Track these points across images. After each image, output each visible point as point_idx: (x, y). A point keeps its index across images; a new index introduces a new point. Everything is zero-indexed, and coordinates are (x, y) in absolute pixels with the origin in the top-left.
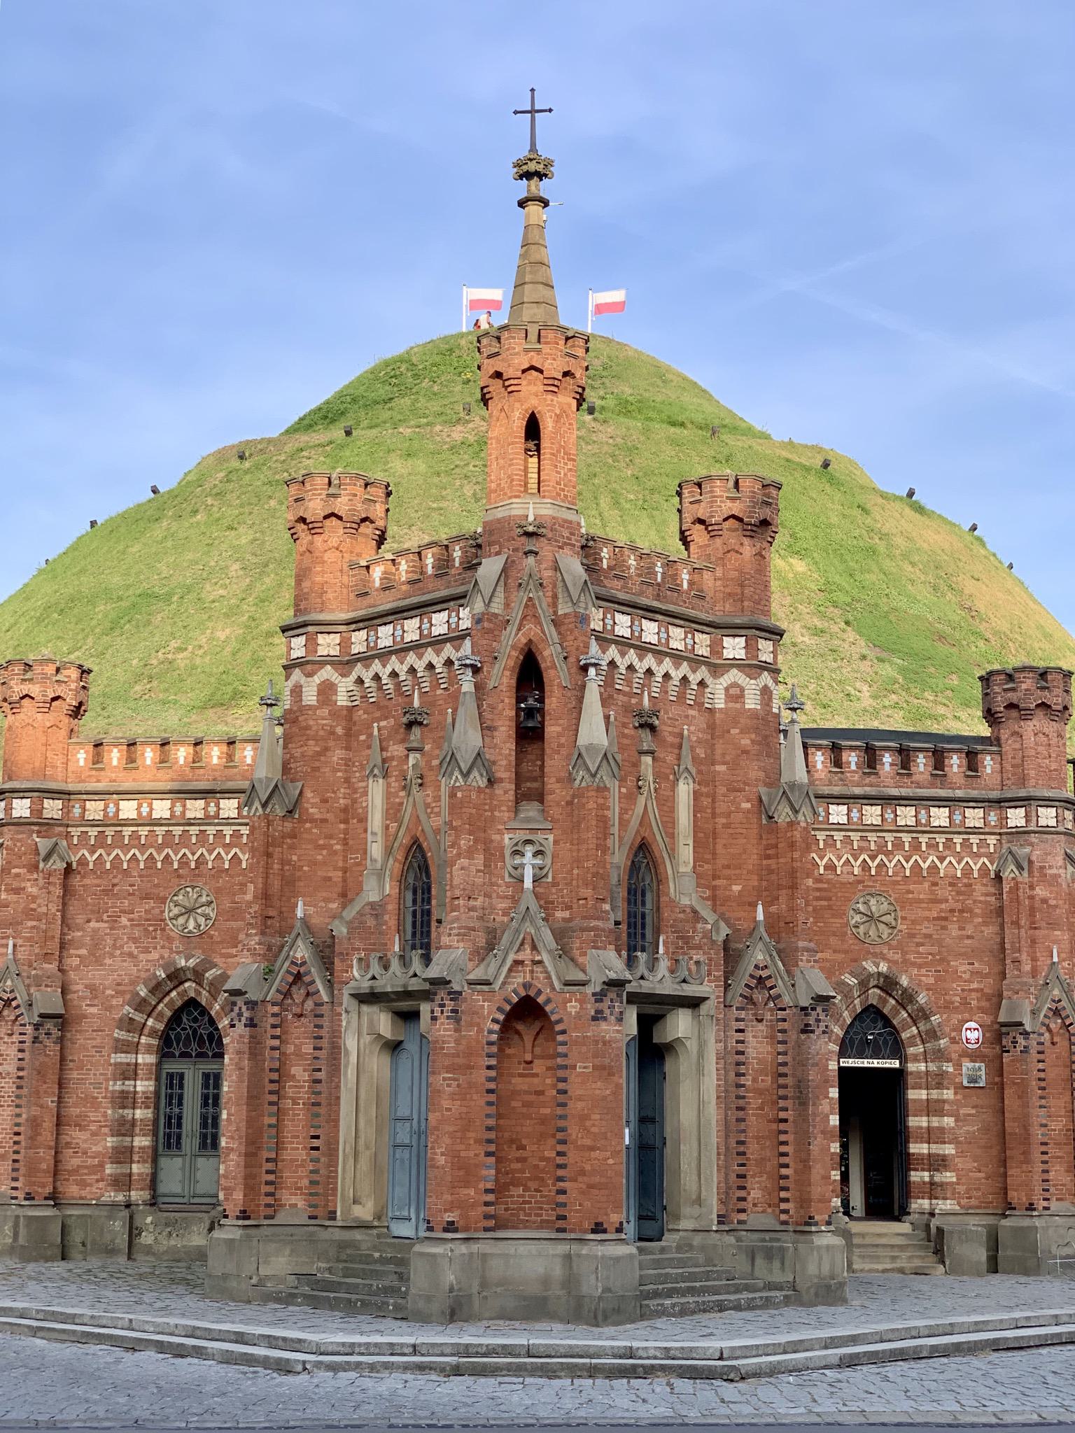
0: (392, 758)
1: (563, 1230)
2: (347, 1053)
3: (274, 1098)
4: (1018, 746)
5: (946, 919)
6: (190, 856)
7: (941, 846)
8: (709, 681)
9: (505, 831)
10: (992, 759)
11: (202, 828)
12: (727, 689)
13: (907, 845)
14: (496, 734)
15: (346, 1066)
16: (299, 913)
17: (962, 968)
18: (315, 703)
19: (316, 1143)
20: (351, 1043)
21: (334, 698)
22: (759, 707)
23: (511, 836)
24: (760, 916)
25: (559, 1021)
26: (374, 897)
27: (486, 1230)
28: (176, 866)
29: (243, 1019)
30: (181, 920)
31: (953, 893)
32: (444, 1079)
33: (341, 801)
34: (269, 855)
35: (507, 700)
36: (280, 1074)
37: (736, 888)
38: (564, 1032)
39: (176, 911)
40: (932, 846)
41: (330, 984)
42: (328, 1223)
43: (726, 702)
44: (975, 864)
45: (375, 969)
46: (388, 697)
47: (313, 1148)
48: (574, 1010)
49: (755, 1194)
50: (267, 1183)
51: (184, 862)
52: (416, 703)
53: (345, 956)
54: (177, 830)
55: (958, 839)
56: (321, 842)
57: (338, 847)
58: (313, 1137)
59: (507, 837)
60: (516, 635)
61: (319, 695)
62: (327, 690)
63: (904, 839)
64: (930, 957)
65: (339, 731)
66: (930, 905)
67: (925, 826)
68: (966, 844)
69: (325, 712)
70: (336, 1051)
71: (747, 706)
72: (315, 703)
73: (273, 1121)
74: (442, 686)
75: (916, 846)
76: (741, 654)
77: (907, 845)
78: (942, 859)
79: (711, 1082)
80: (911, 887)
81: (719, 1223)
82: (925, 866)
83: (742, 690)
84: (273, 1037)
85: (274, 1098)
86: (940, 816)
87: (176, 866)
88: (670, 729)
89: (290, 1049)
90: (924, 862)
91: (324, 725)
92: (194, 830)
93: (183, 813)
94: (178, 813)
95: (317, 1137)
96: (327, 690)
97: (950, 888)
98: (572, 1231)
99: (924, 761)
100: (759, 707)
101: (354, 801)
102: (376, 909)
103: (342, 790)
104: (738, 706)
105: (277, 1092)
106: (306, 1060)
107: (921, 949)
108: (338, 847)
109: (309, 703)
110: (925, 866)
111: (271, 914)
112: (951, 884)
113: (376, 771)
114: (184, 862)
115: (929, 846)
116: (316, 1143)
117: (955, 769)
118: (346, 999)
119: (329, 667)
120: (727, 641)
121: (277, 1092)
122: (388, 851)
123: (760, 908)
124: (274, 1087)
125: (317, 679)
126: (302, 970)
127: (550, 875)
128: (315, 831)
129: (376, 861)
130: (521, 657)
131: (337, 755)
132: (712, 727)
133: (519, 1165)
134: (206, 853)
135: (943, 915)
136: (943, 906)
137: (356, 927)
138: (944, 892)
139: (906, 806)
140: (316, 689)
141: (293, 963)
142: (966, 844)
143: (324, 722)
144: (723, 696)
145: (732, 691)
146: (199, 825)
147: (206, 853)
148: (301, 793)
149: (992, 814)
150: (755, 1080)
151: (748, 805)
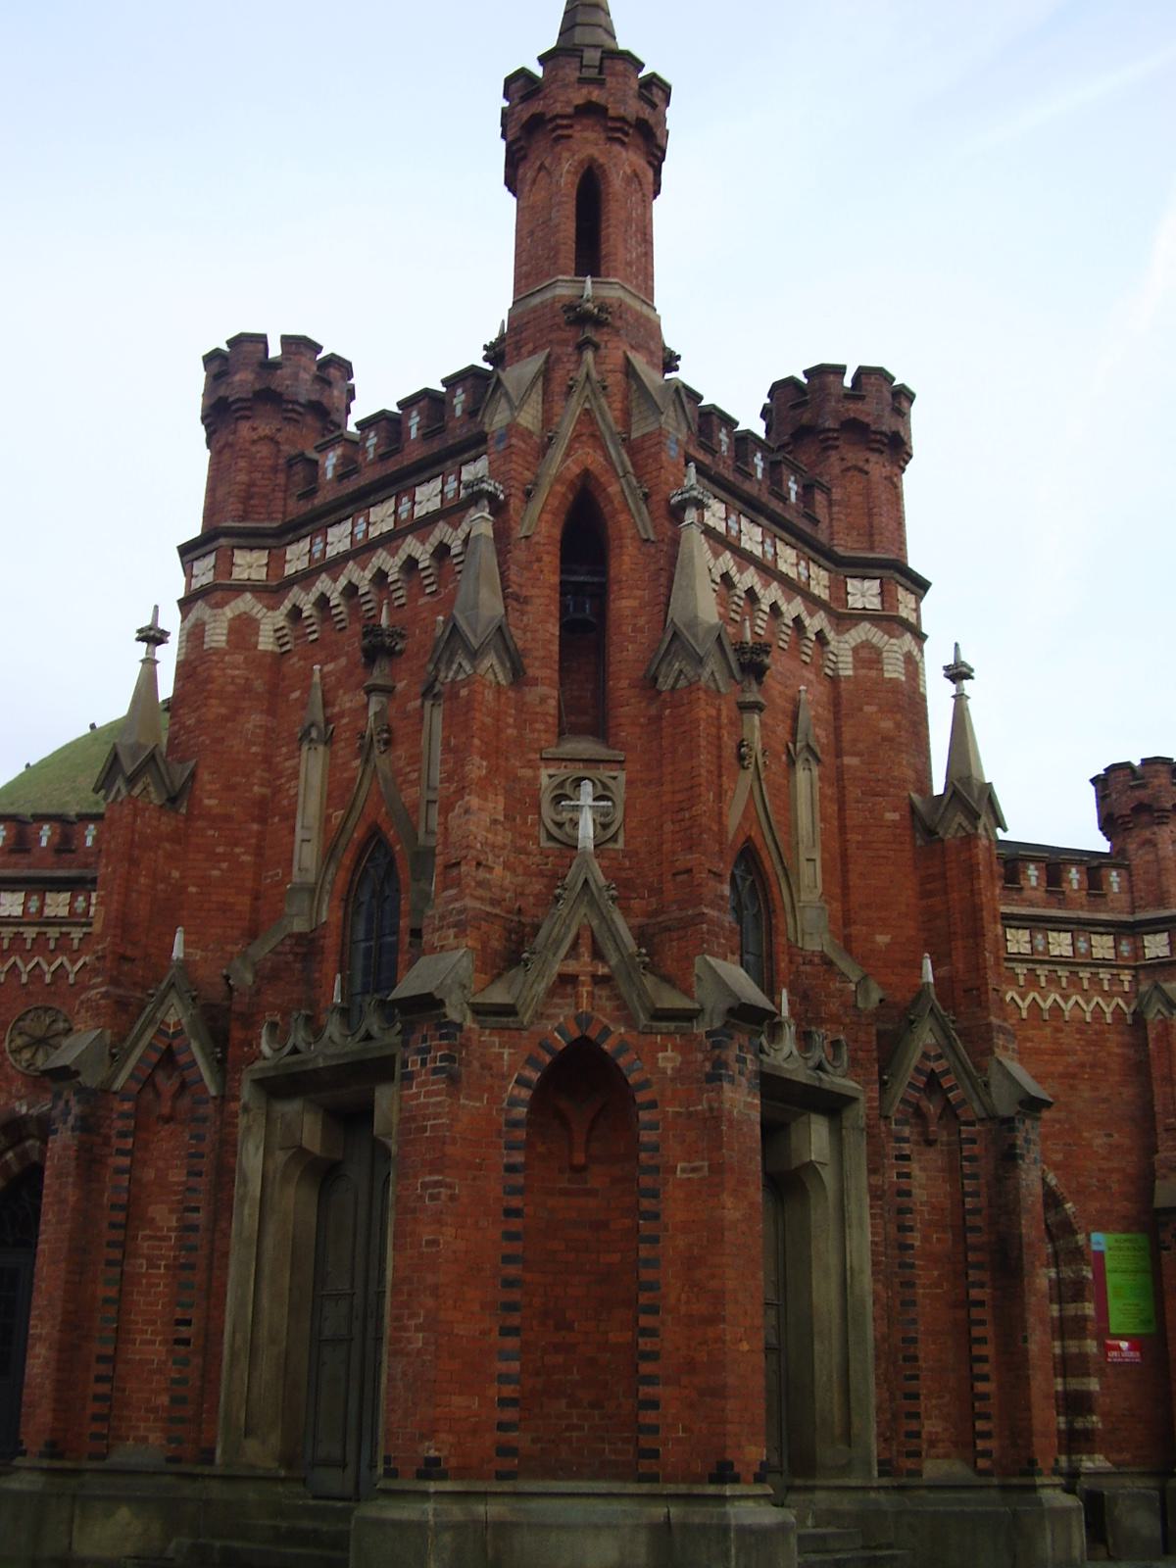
0: (341, 715)
1: (653, 1478)
2: (245, 1182)
3: (117, 1254)
4: (1151, 857)
5: (1074, 1076)
6: (45, 967)
7: (1064, 980)
8: (830, 635)
9: (542, 764)
10: (1118, 876)
11: (64, 929)
12: (855, 650)
13: (1021, 978)
14: (529, 608)
15: (242, 1201)
16: (178, 952)
18: (223, 645)
19: (184, 1331)
20: (252, 1159)
21: (253, 640)
22: (903, 678)
23: (552, 771)
24: (928, 974)
25: (645, 1084)
26: (299, 926)
27: (501, 1476)
28: (24, 979)
29: (71, 1120)
30: (27, 1055)
31: (1082, 1043)
32: (425, 1186)
33: (256, 788)
34: (134, 862)
35: (546, 558)
36: (132, 1213)
37: (882, 939)
38: (652, 1105)
39: (19, 1041)
40: (1054, 980)
41: (223, 1066)
42: (198, 1470)
43: (855, 668)
44: (1108, 1006)
45: (299, 1036)
46: (339, 626)
47: (177, 1342)
48: (670, 1065)
49: (931, 1426)
50: (97, 1398)
51: (36, 974)
52: (384, 621)
53: (249, 1021)
54: (30, 933)
55: (1085, 974)
56: (220, 850)
57: (246, 858)
58: (179, 1322)
59: (544, 773)
60: (563, 461)
61: (229, 634)
62: (243, 629)
63: (1018, 971)
64: (1058, 1126)
65: (259, 685)
66: (1055, 1058)
67: (1043, 954)
68: (1095, 980)
69: (239, 658)
70: (224, 1174)
71: (887, 675)
72: (223, 645)
73: (112, 1293)
74: (428, 591)
76: (874, 603)
78: (1066, 998)
79: (862, 1240)
80: (1031, 1033)
81: (881, 1474)
82: (1046, 1005)
83: (878, 652)
84: (121, 1152)
85: (117, 1254)
86: (1061, 944)
87: (24, 979)
88: (779, 687)
89: (150, 1174)
90: (1045, 1001)
91: (233, 677)
92: (53, 932)
93: (41, 910)
94: (33, 910)
95: (188, 1323)
96: (243, 629)
97: (1078, 1036)
98: (668, 1479)
99: (1036, 873)
100: (903, 678)
101: (277, 791)
102: (307, 946)
103: (258, 773)
104: (873, 673)
105: (122, 1245)
106: (176, 1193)
108: (246, 858)
109: (214, 645)
110: (1046, 1005)
111: (129, 953)
112: (1080, 1031)
113: (314, 734)
114: (36, 974)
115: (1049, 980)
116: (184, 1331)
118: (246, 1092)
119: (248, 596)
120: (853, 585)
121: (122, 1245)
122: (329, 854)
123: (928, 965)
124: (118, 1235)
125: (229, 612)
126: (176, 1043)
127: (621, 839)
128: (210, 832)
129: (307, 870)
130: (571, 497)
131: (254, 721)
132: (836, 702)
133: (560, 1359)
134: (67, 964)
135: (1070, 1069)
136: (1070, 1059)
137: (269, 976)
138: (1068, 1039)
139: (1018, 928)
140: (226, 625)
141: (161, 1032)
142: (1095, 980)
143: (237, 672)
144: (850, 659)
145: (864, 654)
146: (61, 925)
147: (67, 964)
148: (193, 775)
149: (1124, 942)
150: (926, 1239)
151: (895, 816)
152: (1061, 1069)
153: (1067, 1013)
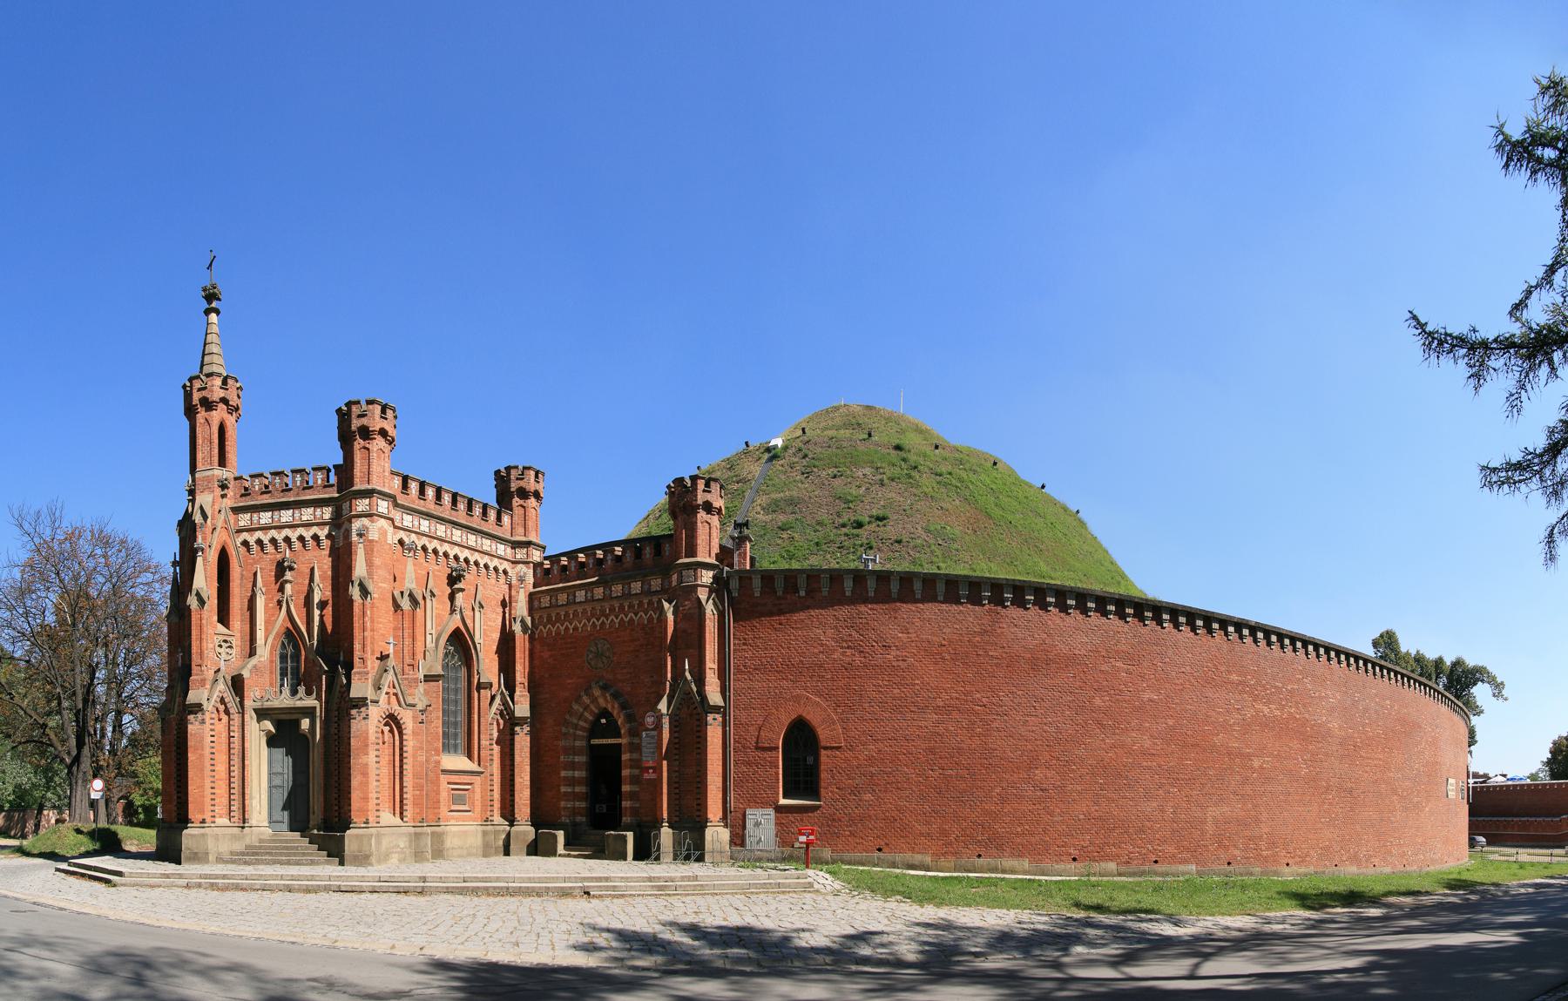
5: (638, 651)
13: (617, 609)
17: (647, 680)
75: (622, 608)
82: (626, 620)
107: (625, 671)
110: (626, 620)
115: (629, 607)
117: (648, 556)
152: (631, 649)
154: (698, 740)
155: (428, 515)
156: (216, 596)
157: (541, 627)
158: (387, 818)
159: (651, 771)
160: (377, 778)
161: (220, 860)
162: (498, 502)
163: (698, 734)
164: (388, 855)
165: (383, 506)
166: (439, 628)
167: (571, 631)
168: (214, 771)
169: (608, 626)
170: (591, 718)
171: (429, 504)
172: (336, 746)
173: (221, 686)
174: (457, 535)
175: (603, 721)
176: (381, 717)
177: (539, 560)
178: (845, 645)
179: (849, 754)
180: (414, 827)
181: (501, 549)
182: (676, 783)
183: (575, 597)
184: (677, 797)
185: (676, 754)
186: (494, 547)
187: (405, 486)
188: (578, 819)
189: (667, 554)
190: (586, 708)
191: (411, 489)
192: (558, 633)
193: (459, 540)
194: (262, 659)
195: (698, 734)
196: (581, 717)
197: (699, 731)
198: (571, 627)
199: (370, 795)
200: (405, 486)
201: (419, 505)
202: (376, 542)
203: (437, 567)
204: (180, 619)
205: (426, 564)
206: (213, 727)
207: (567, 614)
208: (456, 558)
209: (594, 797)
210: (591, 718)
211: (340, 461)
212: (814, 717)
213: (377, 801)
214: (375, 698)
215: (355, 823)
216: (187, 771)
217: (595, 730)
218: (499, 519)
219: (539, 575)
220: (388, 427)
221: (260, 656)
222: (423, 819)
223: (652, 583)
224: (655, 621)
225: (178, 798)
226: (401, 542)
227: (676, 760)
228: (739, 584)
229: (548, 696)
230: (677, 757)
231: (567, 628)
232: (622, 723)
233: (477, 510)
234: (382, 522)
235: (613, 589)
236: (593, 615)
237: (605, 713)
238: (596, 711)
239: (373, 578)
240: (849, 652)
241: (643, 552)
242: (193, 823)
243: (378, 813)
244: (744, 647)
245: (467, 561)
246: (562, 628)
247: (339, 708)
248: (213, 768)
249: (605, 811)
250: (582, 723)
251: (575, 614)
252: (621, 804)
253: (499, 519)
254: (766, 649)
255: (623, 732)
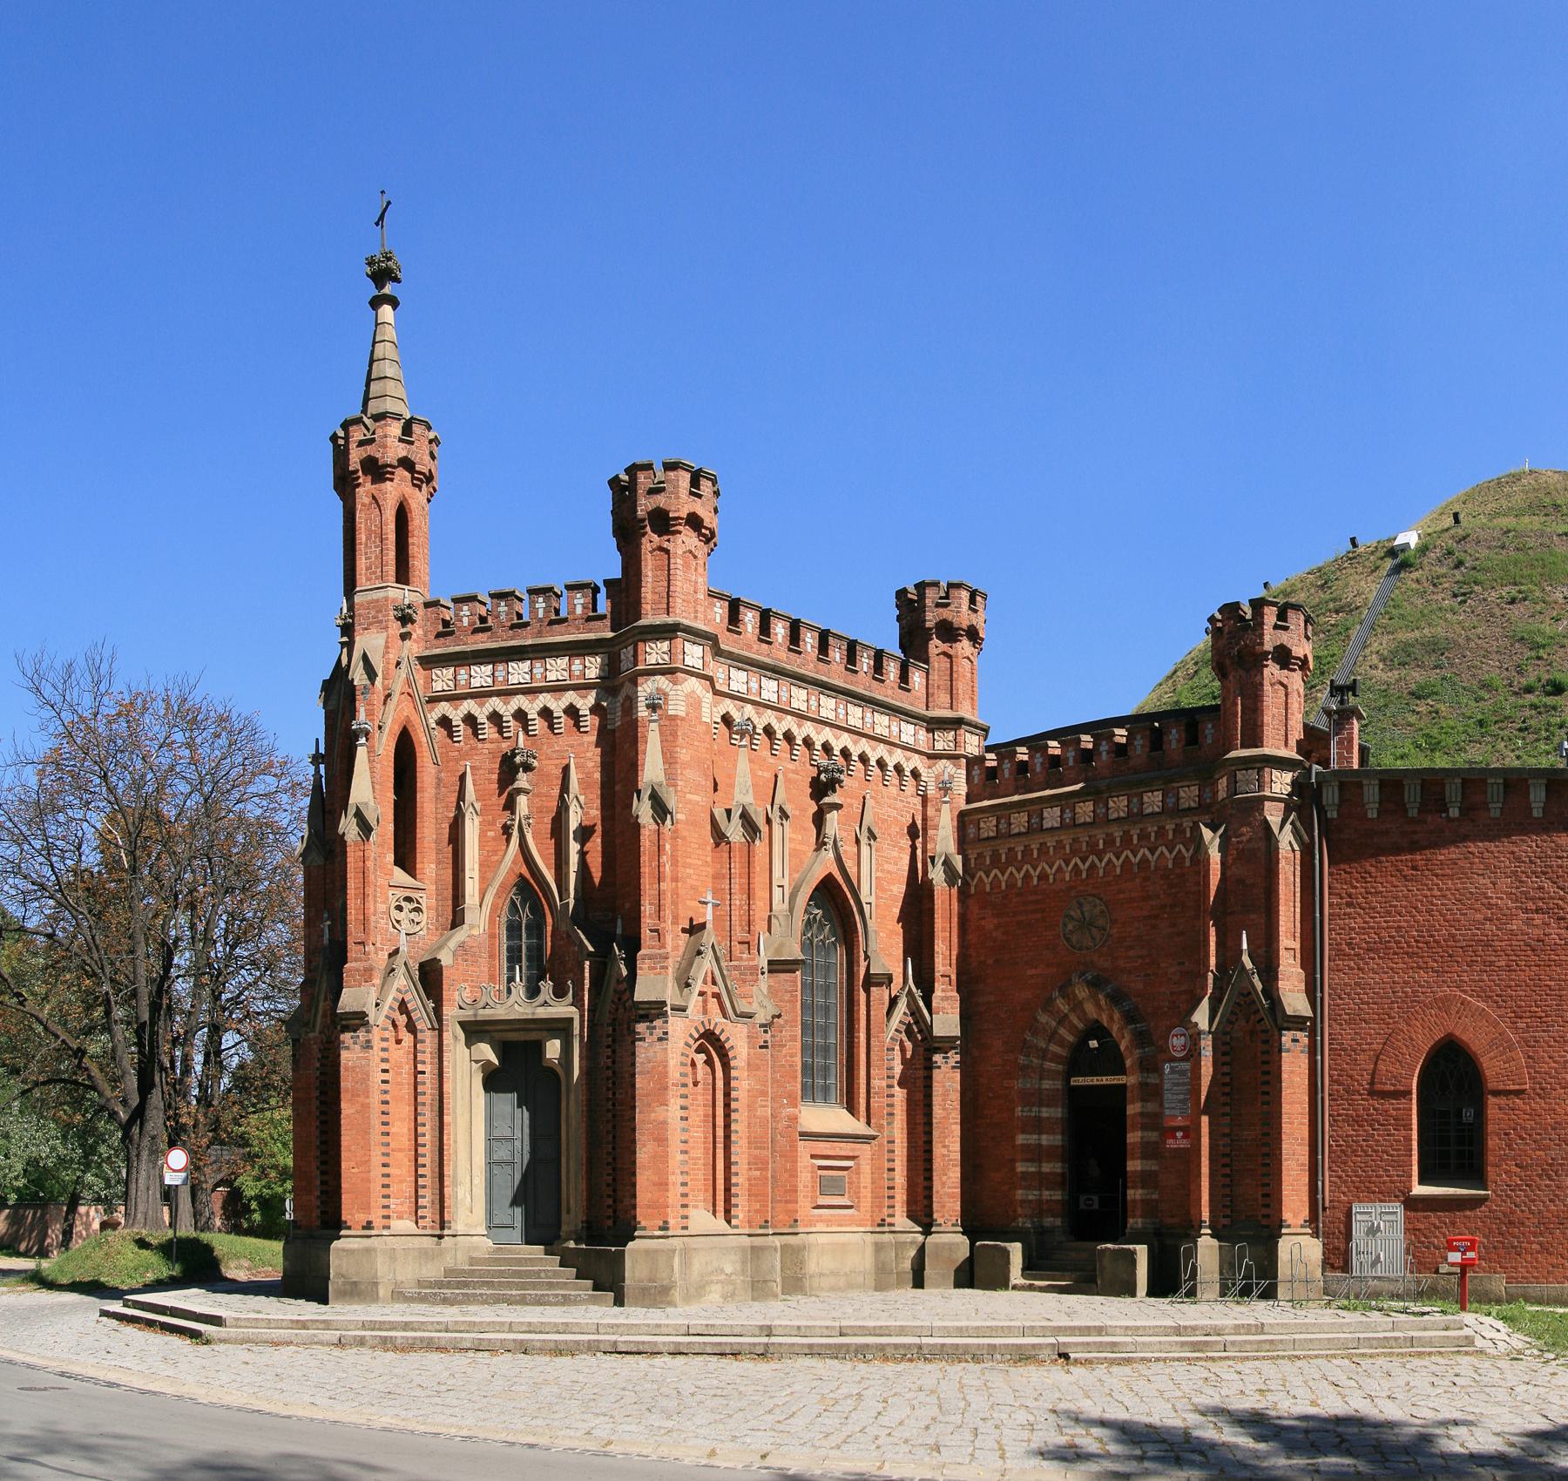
5: (1156, 917)
17: (1172, 970)
75: (1127, 839)
77: (1118, 840)
78: (1152, 852)
90: (1135, 856)
107: (1131, 953)
117: (1174, 745)
136: (1154, 903)
152: (1145, 913)
153: (1153, 864)
154: (1265, 1078)
155: (776, 672)
156: (391, 817)
157: (981, 873)
158: (702, 1219)
159: (1179, 1134)
160: (684, 1147)
161: (398, 1296)
162: (902, 646)
163: (1265, 1067)
164: (703, 1287)
165: (694, 654)
166: (796, 876)
167: (1035, 882)
168: (388, 1134)
169: (1101, 874)
170: (1071, 1038)
171: (778, 651)
172: (608, 1089)
173: (400, 980)
174: (828, 706)
175: (1094, 1044)
176: (691, 1036)
177: (976, 752)
178: (1530, 905)
179: (1538, 1104)
180: (749, 1235)
181: (909, 733)
182: (1224, 1155)
183: (1042, 819)
184: (1228, 1180)
185: (1225, 1104)
186: (895, 729)
187: (734, 618)
188: (1048, 1221)
189: (1209, 741)
190: (1062, 1020)
191: (745, 624)
192: (1011, 884)
193: (832, 716)
194: (475, 932)
195: (1265, 1067)
196: (1052, 1036)
197: (1267, 1062)
198: (1035, 874)
199: (671, 1178)
200: (734, 618)
201: (760, 653)
202: (683, 719)
203: (791, 766)
204: (326, 859)
205: (772, 760)
206: (385, 1054)
207: (1027, 851)
208: (827, 748)
209: (1076, 1181)
210: (1071, 1038)
211: (617, 573)
212: (1475, 1037)
213: (682, 1190)
214: (679, 1002)
215: (644, 1228)
216: (339, 1135)
217: (1079, 1060)
218: (904, 677)
219: (976, 781)
220: (702, 510)
221: (472, 927)
222: (767, 1222)
223: (1182, 794)
224: (1188, 864)
225: (323, 1183)
226: (727, 720)
227: (1223, 1114)
228: (1340, 794)
229: (992, 999)
230: (1227, 1109)
231: (1027, 876)
232: (1127, 1047)
233: (865, 662)
234: (693, 684)
235: (1111, 804)
236: (1074, 852)
237: (1097, 1030)
238: (1081, 1026)
239: (675, 786)
240: (1538, 919)
241: (1165, 738)
242: (349, 1228)
243: (685, 1211)
244: (1348, 910)
245: (845, 753)
246: (1019, 876)
247: (614, 1020)
248: (385, 1129)
249: (1096, 1206)
250: (1054, 1048)
251: (1043, 849)
252: (1125, 1194)
253: (904, 677)
254: (1389, 913)
255: (1128, 1063)
